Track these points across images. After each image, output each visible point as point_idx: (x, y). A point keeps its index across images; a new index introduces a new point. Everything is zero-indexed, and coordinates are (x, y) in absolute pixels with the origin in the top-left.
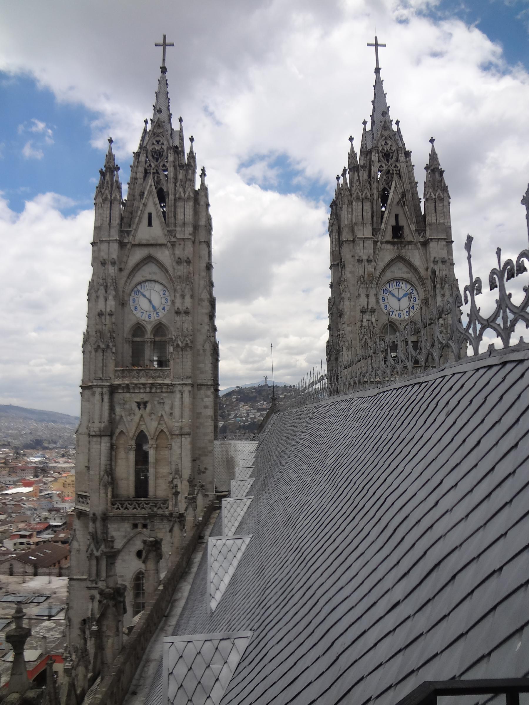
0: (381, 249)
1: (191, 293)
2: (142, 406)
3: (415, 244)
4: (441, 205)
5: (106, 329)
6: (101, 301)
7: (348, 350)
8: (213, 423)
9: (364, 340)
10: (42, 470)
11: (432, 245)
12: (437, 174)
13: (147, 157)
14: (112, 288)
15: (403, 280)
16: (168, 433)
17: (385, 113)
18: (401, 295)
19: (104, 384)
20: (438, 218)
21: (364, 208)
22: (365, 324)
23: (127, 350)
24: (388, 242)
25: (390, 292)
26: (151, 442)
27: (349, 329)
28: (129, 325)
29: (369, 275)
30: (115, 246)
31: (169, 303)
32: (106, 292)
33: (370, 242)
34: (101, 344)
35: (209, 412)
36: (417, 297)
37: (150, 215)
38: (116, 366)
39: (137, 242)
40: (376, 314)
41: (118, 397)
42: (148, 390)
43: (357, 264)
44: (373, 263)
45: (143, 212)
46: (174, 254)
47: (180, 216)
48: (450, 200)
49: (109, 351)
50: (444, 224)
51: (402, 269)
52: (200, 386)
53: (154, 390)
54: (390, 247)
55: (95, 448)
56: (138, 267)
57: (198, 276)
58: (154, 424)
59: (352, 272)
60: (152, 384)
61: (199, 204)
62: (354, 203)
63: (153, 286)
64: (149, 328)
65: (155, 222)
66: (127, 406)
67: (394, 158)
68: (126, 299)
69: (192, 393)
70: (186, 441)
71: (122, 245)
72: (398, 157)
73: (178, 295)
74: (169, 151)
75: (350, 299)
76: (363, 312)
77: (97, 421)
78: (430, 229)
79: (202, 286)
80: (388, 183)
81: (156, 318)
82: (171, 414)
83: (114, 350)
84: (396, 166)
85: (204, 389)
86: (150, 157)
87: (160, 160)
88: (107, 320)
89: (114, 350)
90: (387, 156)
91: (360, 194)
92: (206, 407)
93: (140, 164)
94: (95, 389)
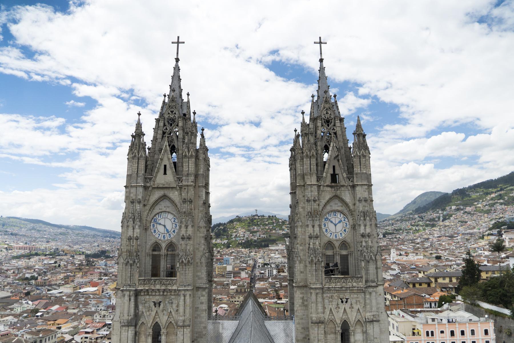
0: (323, 191)
1: (192, 224)
2: (157, 305)
3: (347, 187)
4: (364, 160)
5: (134, 249)
6: (131, 229)
7: (300, 262)
8: (207, 315)
9: (311, 258)
10: (104, 274)
11: (358, 189)
12: (361, 138)
13: (164, 124)
14: (138, 220)
15: (339, 211)
16: (175, 324)
17: (326, 92)
18: (337, 222)
19: (131, 289)
20: (362, 169)
21: (312, 162)
22: (311, 246)
23: (148, 262)
24: (327, 186)
25: (329, 220)
26: (163, 331)
27: (301, 248)
28: (150, 243)
29: (314, 211)
30: (141, 190)
31: (178, 228)
32: (134, 223)
33: (316, 187)
34: (129, 260)
35: (205, 307)
36: (348, 223)
37: (165, 166)
38: (140, 276)
39: (156, 186)
40: (319, 239)
41: (141, 298)
42: (161, 293)
43: (306, 203)
44: (317, 202)
45: (160, 164)
46: (181, 194)
47: (185, 169)
48: (370, 156)
49: (135, 265)
50: (366, 173)
51: (337, 204)
52: (198, 288)
53: (165, 294)
54: (329, 189)
55: (124, 334)
56: (156, 202)
57: (197, 210)
58: (166, 318)
59: (303, 208)
60: (164, 291)
61: (199, 159)
62: (305, 159)
63: (167, 215)
64: (164, 245)
65: (169, 172)
66: (147, 305)
67: (333, 124)
68: (148, 225)
69: (192, 296)
70: (187, 331)
71: (145, 188)
72: (335, 123)
73: (183, 226)
74: (179, 119)
75: (301, 226)
76: (310, 237)
77: (126, 315)
78: (357, 177)
79: (200, 217)
80: (329, 142)
81: (169, 238)
82: (177, 310)
83: (138, 265)
84: (334, 129)
85: (201, 290)
86: (167, 123)
87: (173, 125)
88: (134, 243)
89: (138, 265)
90: (328, 122)
91: (308, 153)
92: (202, 303)
93: (159, 129)
94: (124, 292)
